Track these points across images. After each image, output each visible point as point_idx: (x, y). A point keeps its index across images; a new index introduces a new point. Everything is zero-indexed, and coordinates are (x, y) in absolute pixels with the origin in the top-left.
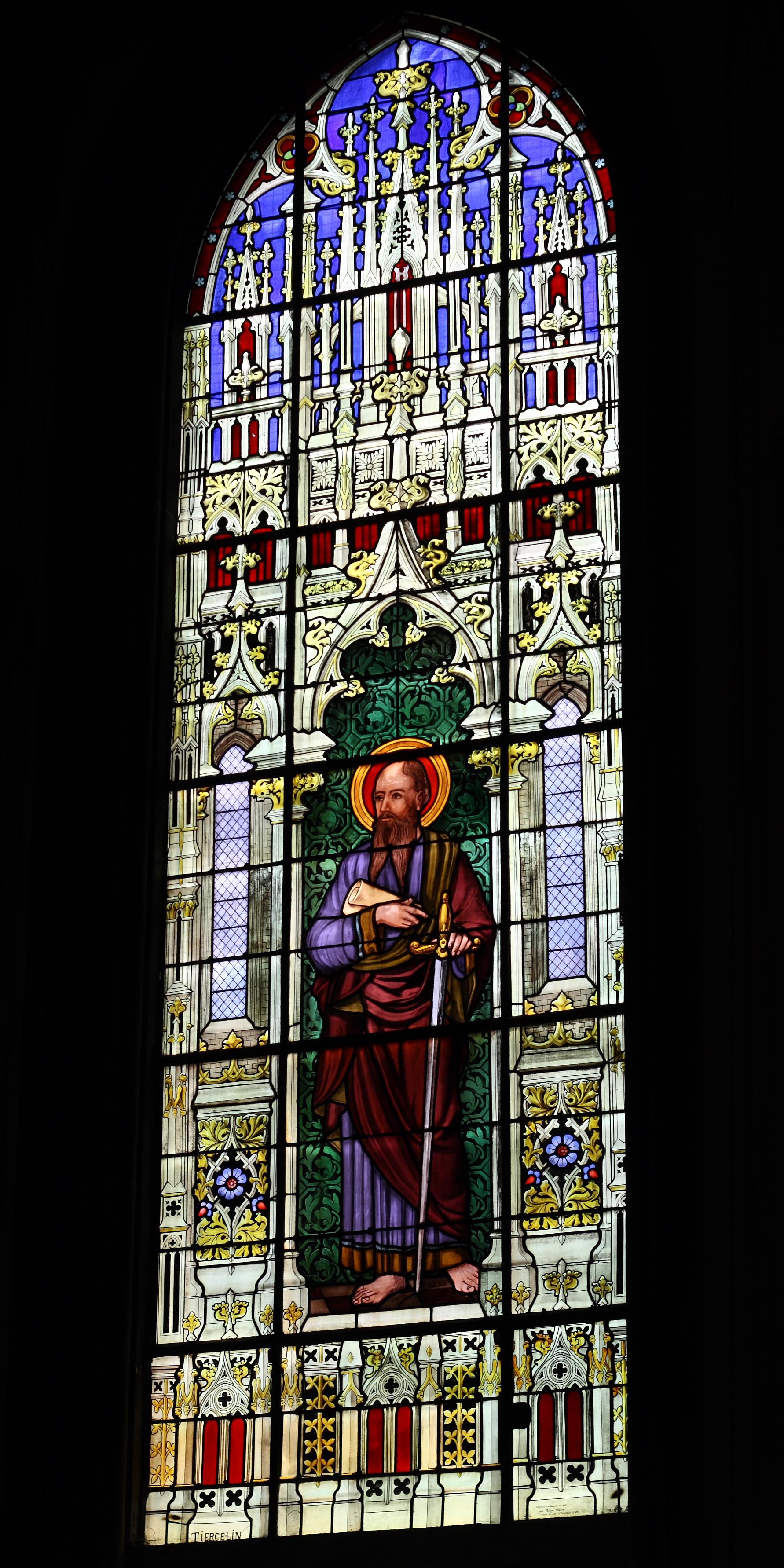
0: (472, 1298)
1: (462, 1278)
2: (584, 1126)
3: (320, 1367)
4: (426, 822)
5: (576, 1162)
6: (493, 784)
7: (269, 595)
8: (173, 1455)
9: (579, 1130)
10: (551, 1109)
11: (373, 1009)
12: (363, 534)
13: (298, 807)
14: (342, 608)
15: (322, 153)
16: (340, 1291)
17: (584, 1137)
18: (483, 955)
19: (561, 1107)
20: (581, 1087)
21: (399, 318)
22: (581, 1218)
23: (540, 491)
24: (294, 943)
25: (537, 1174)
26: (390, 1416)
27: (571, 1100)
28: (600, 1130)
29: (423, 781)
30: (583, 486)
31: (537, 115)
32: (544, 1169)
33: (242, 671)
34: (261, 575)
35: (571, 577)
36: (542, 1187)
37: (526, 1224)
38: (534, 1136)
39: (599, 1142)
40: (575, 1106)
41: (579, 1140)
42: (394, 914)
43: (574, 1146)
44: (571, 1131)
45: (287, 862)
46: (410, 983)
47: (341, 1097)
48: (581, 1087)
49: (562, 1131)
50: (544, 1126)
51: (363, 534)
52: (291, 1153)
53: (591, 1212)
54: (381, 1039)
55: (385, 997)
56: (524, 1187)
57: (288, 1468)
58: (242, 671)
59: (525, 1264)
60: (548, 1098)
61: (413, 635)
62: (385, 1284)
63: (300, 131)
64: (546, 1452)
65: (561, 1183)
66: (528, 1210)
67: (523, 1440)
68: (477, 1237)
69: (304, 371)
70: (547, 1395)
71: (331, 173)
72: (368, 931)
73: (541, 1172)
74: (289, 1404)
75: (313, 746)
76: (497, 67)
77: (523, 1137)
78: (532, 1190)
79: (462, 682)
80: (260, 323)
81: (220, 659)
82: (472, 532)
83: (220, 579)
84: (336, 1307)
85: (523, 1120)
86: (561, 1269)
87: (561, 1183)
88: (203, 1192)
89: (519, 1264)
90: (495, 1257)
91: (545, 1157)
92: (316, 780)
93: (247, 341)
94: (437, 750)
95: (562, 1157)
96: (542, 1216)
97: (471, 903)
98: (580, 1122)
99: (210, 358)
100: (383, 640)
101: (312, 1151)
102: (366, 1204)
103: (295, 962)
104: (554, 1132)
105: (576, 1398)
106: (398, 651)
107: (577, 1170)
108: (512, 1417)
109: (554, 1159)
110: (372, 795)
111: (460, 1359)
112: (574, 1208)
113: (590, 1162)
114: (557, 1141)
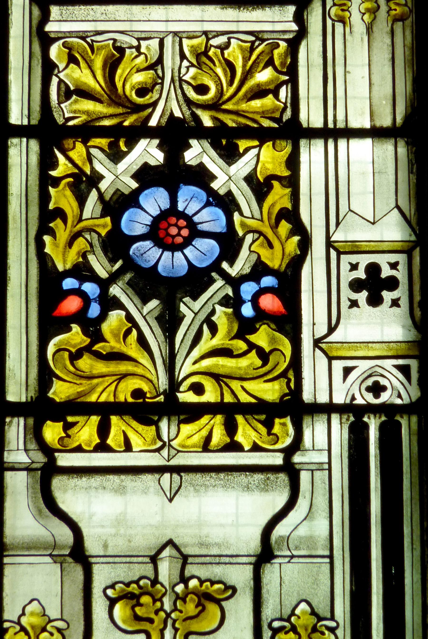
2: (243, 166)
5: (216, 266)
9: (228, 177)
10: (137, 108)
17: (244, 197)
19: (168, 105)
20: (235, 54)
22: (231, 428)
25: (90, 288)
27: (202, 89)
28: (292, 182)
32: (114, 278)
36: (106, 328)
37: (52, 432)
38: (84, 183)
39: (291, 215)
40: (214, 106)
41: (227, 203)
43: (211, 219)
44: (200, 176)
48: (235, 54)
49: (172, 175)
50: (116, 156)
53: (265, 412)
56: (50, 324)
59: (51, 550)
60: (131, 78)
65: (170, 322)
66: (60, 391)
73: (104, 285)
77: (46, 181)
78: (76, 336)
85: (50, 134)
86: (166, 570)
87: (170, 322)
89: (32, 547)
91: (117, 244)
95: (174, 248)
96: (105, 411)
98: (230, 155)
104: (146, 176)
107: (218, 287)
109: (147, 253)
112: (210, 395)
113: (259, 270)
114: (155, 201)
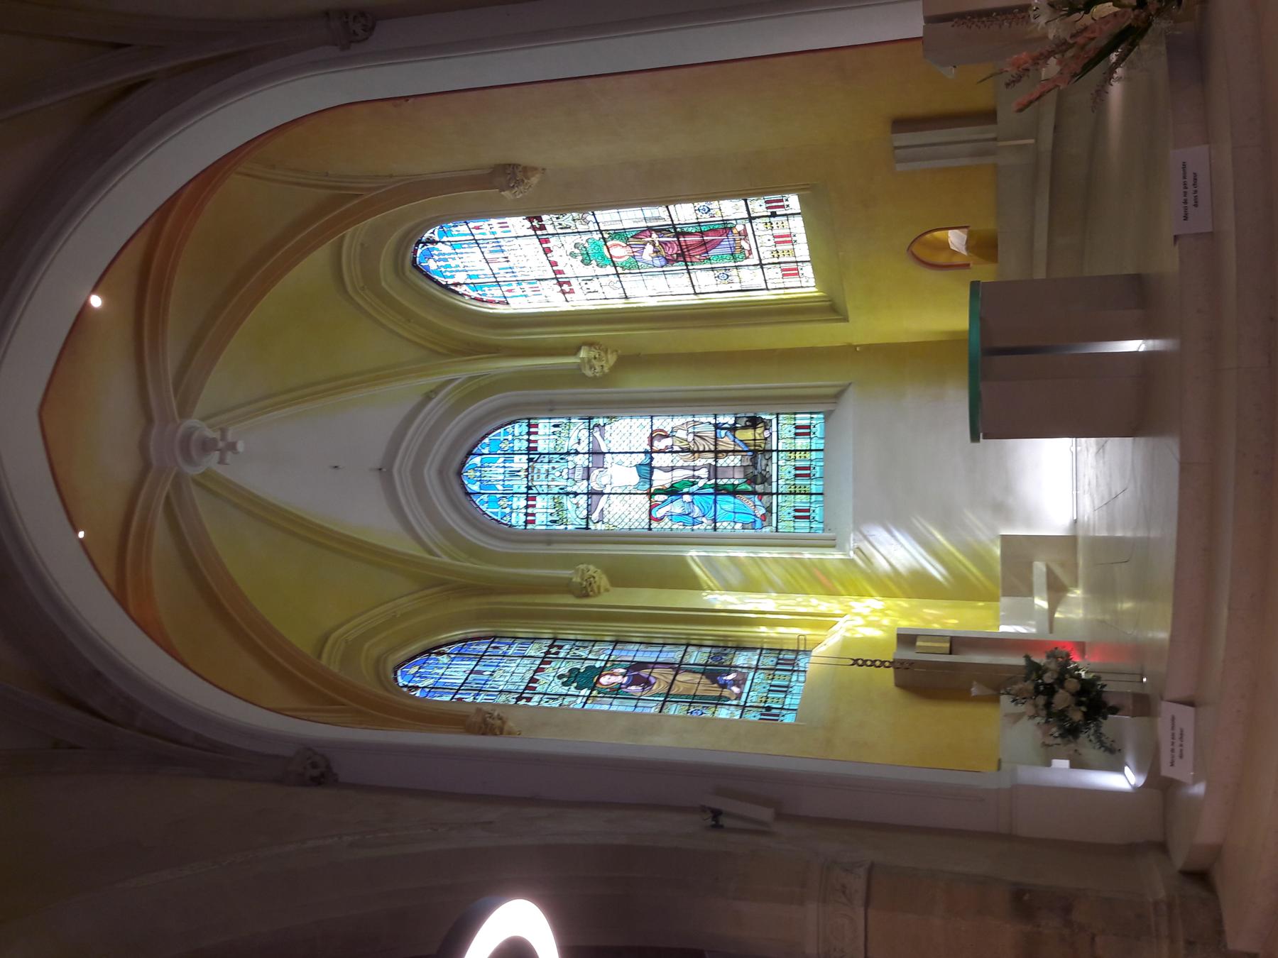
1: (740, 228)
3: (768, 255)
12: (553, 264)
14: (573, 268)
15: (455, 280)
21: (495, 261)
34: (569, 283)
42: (649, 248)
51: (553, 264)
61: (577, 251)
62: (743, 243)
64: (783, 207)
67: (779, 211)
71: (460, 278)
74: (776, 260)
75: (611, 270)
82: (547, 241)
84: (750, 252)
108: (774, 215)
111: (762, 227)
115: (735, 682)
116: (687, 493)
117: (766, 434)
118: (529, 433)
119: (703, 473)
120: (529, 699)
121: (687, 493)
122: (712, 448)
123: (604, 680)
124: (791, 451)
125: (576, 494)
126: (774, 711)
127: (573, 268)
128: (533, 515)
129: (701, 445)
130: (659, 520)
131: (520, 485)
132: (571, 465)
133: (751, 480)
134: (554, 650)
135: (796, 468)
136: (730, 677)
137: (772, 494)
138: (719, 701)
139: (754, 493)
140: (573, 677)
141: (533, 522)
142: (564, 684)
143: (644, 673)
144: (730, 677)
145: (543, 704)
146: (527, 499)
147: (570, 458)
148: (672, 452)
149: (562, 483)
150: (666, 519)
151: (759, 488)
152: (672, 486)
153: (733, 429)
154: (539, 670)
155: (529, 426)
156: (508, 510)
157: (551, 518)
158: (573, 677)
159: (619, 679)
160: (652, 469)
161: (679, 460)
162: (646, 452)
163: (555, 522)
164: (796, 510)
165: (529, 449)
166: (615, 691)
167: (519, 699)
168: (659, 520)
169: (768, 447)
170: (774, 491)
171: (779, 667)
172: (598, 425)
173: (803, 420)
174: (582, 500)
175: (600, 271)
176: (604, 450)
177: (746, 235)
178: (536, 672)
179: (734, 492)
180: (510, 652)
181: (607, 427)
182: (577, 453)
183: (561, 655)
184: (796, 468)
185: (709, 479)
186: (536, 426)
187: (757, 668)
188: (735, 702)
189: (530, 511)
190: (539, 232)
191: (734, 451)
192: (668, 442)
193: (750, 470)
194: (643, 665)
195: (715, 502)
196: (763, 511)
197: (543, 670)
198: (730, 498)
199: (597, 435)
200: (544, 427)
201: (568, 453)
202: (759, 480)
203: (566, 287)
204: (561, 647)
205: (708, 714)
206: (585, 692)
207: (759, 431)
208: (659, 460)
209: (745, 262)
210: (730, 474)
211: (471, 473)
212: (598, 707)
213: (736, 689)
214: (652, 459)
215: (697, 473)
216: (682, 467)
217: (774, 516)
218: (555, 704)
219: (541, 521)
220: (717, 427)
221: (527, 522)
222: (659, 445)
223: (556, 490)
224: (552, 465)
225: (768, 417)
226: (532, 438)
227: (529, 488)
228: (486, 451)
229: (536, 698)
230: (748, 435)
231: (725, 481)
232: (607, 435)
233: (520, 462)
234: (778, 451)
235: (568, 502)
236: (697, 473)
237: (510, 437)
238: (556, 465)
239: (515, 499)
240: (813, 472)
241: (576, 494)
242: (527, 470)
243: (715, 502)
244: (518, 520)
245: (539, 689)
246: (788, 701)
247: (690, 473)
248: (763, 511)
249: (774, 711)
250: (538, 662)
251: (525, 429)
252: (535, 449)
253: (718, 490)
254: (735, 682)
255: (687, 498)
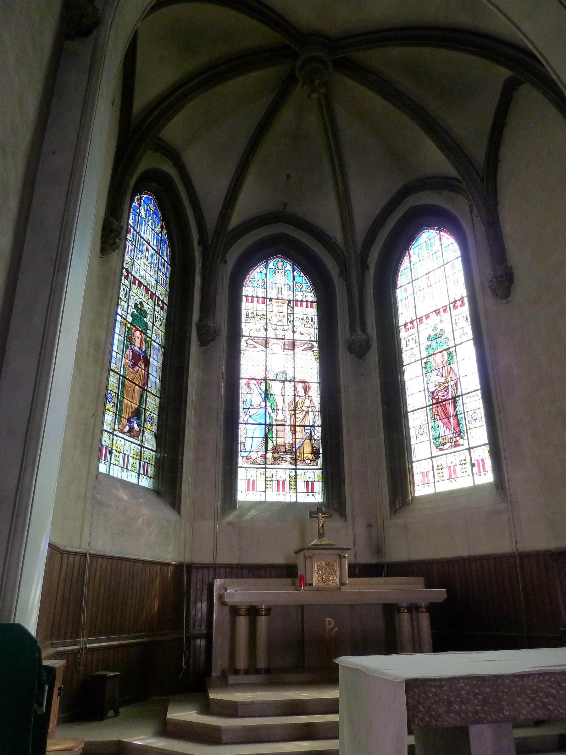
0: (463, 445)
1: (461, 442)
4: (444, 363)
6: (454, 354)
7: (415, 330)
8: (418, 479)
11: (440, 397)
12: (427, 317)
13: (424, 365)
14: (426, 329)
15: (412, 255)
16: (441, 447)
18: (456, 384)
23: (455, 302)
24: (426, 388)
26: (452, 468)
29: (443, 356)
30: (462, 298)
31: (446, 238)
33: (412, 344)
34: (413, 328)
35: (462, 315)
45: (423, 375)
46: (445, 391)
47: (437, 413)
51: (427, 317)
52: (430, 424)
54: (442, 402)
55: (442, 395)
57: (436, 480)
58: (412, 344)
61: (438, 331)
63: (409, 253)
64: (479, 472)
67: (475, 469)
68: (462, 434)
69: (415, 292)
70: (478, 461)
71: (413, 258)
72: (438, 384)
74: (435, 468)
75: (424, 354)
76: (438, 232)
79: (447, 338)
80: (407, 286)
81: (408, 343)
83: (406, 330)
84: (441, 450)
88: (417, 433)
90: (466, 437)
92: (425, 360)
93: (406, 290)
94: (444, 350)
97: (454, 375)
99: (400, 294)
100: (433, 333)
101: (433, 423)
102: (444, 431)
103: (426, 391)
105: (483, 460)
106: (436, 335)
108: (473, 465)
110: (435, 360)
115: (131, 430)
116: (266, 406)
117: (308, 462)
118: (307, 301)
119: (280, 417)
120: (126, 277)
121: (266, 406)
122: (297, 424)
123: (138, 333)
124: (296, 478)
125: (266, 330)
126: (108, 456)
127: (426, 329)
128: (252, 301)
129: (300, 416)
130: (248, 385)
131: (273, 293)
132: (286, 328)
133: (275, 450)
134: (160, 303)
135: (283, 482)
136: (136, 426)
137: (265, 464)
138: (118, 416)
139: (266, 451)
140: (141, 312)
141: (247, 301)
142: (136, 305)
143: (141, 364)
144: (136, 426)
145: (123, 287)
146: (263, 298)
147: (291, 327)
148: (295, 395)
149: (275, 320)
150: (248, 390)
151: (269, 455)
152: (271, 395)
153: (310, 438)
154: (147, 290)
155: (312, 302)
156: (255, 284)
157: (250, 312)
158: (141, 312)
159: (138, 344)
160: (283, 381)
161: (289, 398)
162: (294, 378)
163: (248, 315)
164: (254, 481)
165: (297, 301)
166: (129, 339)
167: (127, 271)
168: (248, 385)
169: (298, 462)
170: (267, 466)
171: (142, 463)
172: (313, 346)
173: (319, 487)
174: (262, 334)
175: (423, 348)
176: (295, 350)
177: (455, 446)
178: (146, 287)
179: (266, 437)
180: (160, 274)
181: (312, 353)
182: (294, 332)
183: (157, 308)
184: (283, 482)
185: (276, 420)
186: (312, 307)
187: (142, 446)
188: (117, 427)
189: (255, 299)
190: (452, 305)
191: (295, 438)
192: (302, 393)
193: (283, 450)
194: (147, 363)
195: (261, 424)
196: (254, 457)
197: (147, 293)
198: (263, 435)
199: (306, 346)
200: (312, 312)
201: (294, 326)
202: (276, 455)
203: (409, 326)
204: (162, 308)
205: (109, 406)
206: (130, 319)
207: (310, 456)
208: (289, 386)
209: (433, 447)
210: (281, 434)
211: (280, 264)
212: (118, 325)
213: (127, 428)
214: (290, 381)
215: (280, 412)
216: (284, 402)
217: (251, 466)
218: (122, 295)
219: (246, 307)
220: (313, 426)
221: (247, 296)
222: (300, 387)
223: (269, 317)
224: (286, 315)
225: (319, 463)
226: (304, 304)
227: (271, 299)
228: (295, 273)
229: (127, 283)
230: (307, 449)
231: (275, 432)
232: (306, 352)
233: (287, 295)
234: (296, 469)
235: (260, 324)
236: (280, 412)
237: (304, 289)
238: (286, 318)
239: (263, 290)
240: (281, 494)
241: (266, 330)
242: (282, 299)
243: (261, 424)
244: (247, 290)
245: (134, 287)
246: (116, 468)
247: (280, 408)
248: (254, 457)
249: (108, 456)
250: (153, 290)
251: (310, 299)
252: (297, 305)
253: (268, 427)
254: (131, 430)
255: (263, 404)
